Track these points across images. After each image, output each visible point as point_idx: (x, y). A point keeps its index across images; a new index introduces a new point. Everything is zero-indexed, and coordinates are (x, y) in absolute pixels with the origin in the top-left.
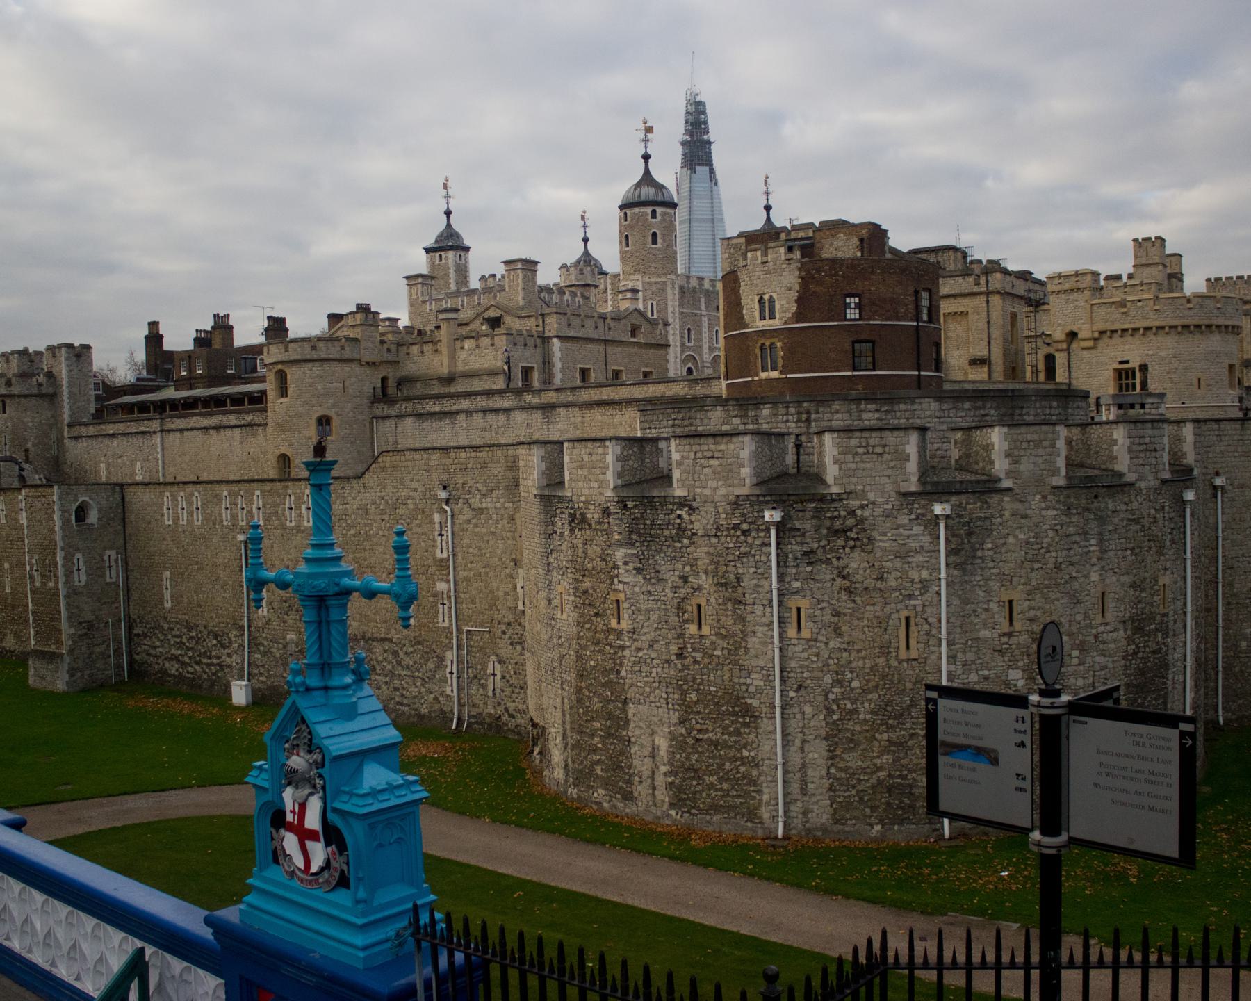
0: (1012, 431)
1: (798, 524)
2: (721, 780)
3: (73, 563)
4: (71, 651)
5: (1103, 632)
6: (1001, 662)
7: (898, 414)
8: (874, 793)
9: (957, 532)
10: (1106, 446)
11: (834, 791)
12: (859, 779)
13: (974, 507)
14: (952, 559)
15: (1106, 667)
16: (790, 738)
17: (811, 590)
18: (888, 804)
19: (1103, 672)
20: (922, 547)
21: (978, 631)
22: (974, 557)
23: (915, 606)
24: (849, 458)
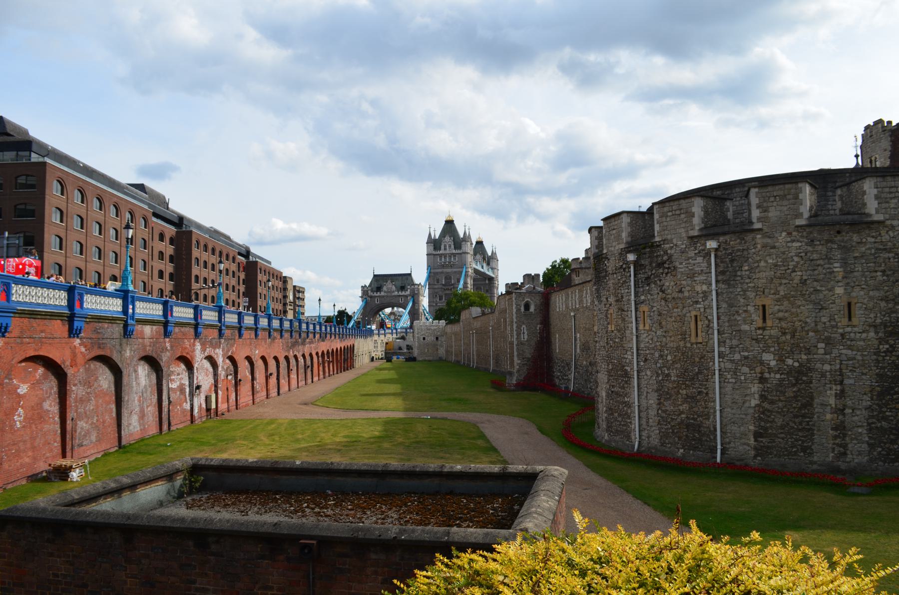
0: (762, 191)
1: (643, 262)
2: (620, 415)
3: (521, 330)
4: (518, 371)
5: (850, 333)
7: (735, 195)
8: (680, 428)
9: (724, 260)
10: (860, 197)
11: (661, 425)
13: (734, 242)
14: (720, 278)
15: (854, 359)
16: (642, 390)
18: (687, 436)
19: (851, 362)
20: (702, 270)
21: (740, 325)
22: (736, 276)
23: (699, 308)
24: (664, 219)
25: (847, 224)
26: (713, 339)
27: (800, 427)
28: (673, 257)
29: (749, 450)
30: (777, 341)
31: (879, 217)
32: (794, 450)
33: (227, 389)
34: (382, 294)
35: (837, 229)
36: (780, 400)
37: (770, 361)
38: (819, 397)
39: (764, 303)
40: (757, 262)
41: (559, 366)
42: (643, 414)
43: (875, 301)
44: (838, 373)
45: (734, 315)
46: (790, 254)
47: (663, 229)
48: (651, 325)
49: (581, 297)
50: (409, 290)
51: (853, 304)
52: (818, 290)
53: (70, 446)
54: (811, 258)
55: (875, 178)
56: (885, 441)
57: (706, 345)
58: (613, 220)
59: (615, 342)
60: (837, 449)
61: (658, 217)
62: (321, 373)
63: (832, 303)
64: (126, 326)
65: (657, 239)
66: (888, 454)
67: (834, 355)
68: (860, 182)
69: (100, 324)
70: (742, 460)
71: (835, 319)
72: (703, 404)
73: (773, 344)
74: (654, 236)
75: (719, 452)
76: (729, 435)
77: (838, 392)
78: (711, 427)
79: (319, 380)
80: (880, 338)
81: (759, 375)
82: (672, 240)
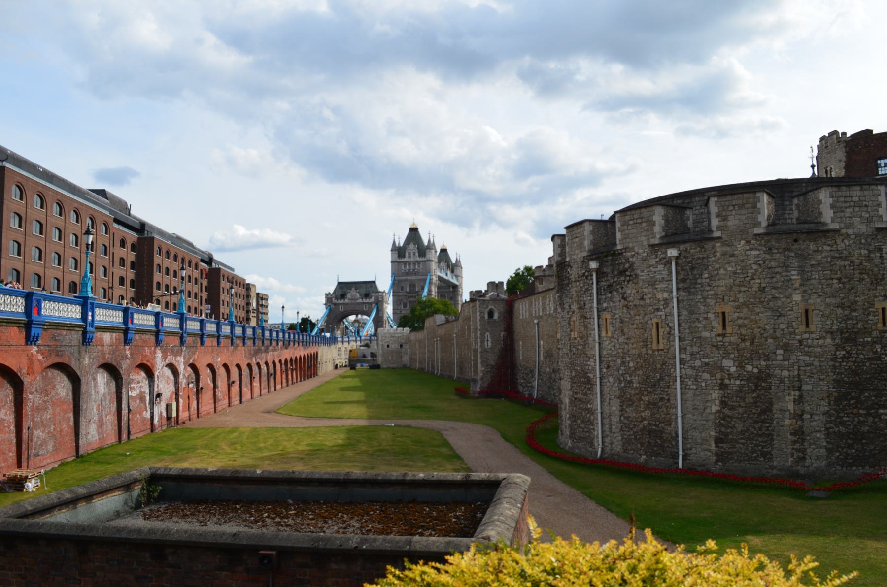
0: (721, 200)
1: (605, 270)
2: (583, 422)
3: (485, 337)
4: (482, 378)
5: (807, 339)
6: (717, 354)
7: (695, 204)
8: (642, 434)
9: (685, 268)
10: (816, 206)
11: (623, 431)
12: (634, 425)
13: (694, 250)
14: (680, 285)
16: (605, 397)
17: (611, 308)
18: (649, 442)
19: (809, 368)
20: (663, 278)
21: (701, 332)
22: (696, 283)
23: (661, 315)
25: (804, 233)
26: (674, 346)
27: (760, 432)
28: (635, 265)
29: (710, 456)
30: (737, 348)
31: (835, 226)
32: (755, 455)
33: (188, 397)
34: (347, 301)
35: (795, 238)
36: (740, 406)
37: (730, 367)
38: (778, 403)
39: (723, 311)
40: (717, 269)
41: (523, 373)
42: (606, 421)
43: (832, 308)
44: (797, 379)
45: (695, 322)
46: (749, 262)
47: (625, 237)
48: (613, 332)
49: (544, 304)
50: (373, 298)
51: (810, 311)
52: (776, 297)
53: (26, 455)
54: (769, 266)
55: (830, 188)
56: (843, 445)
57: (668, 352)
58: (575, 228)
59: (578, 349)
60: (796, 454)
61: (620, 226)
62: (284, 381)
63: (789, 310)
64: (85, 333)
65: (619, 247)
66: (846, 458)
67: (793, 361)
68: (816, 192)
69: (58, 331)
70: (703, 466)
71: (793, 326)
72: (665, 410)
73: (733, 351)
74: (615, 244)
75: (681, 458)
76: (690, 441)
77: (797, 398)
78: (673, 433)
79: (282, 388)
80: (836, 345)
81: (719, 381)
82: (633, 248)
